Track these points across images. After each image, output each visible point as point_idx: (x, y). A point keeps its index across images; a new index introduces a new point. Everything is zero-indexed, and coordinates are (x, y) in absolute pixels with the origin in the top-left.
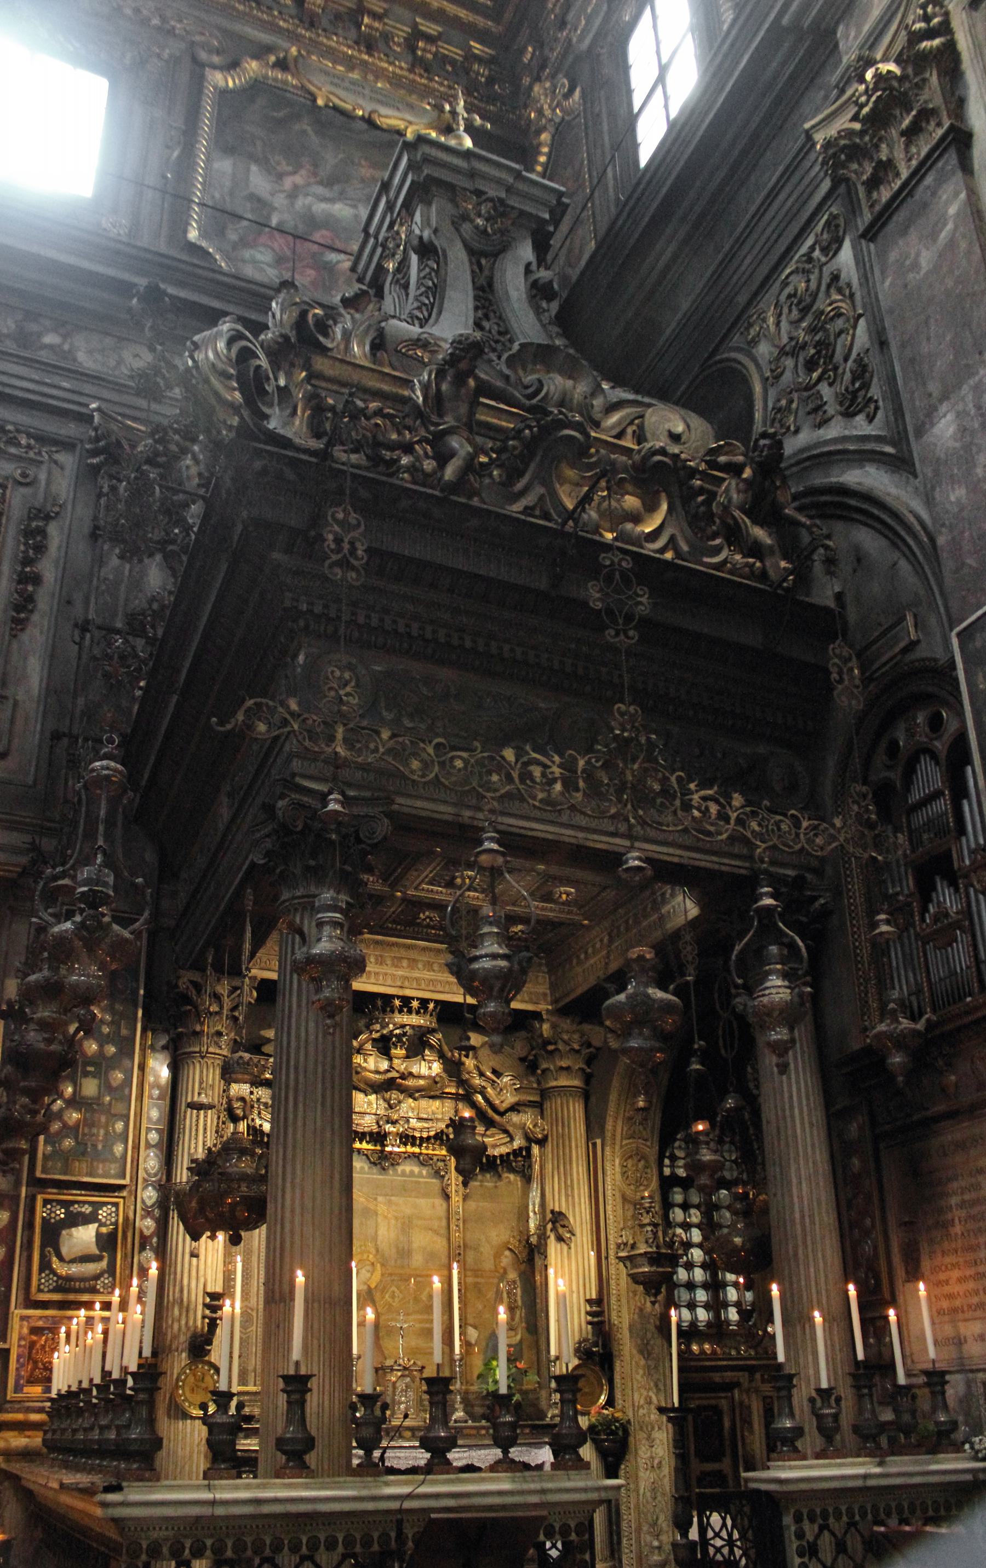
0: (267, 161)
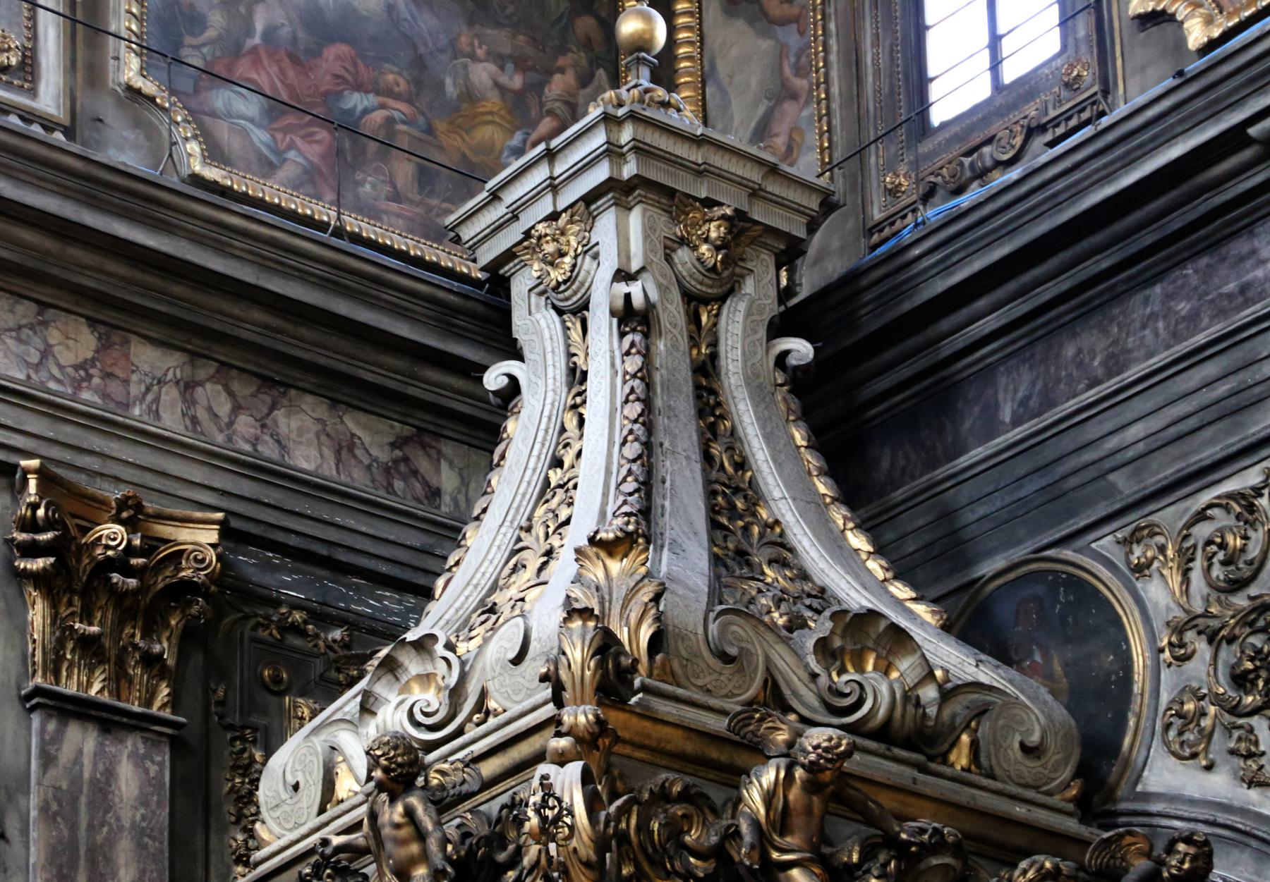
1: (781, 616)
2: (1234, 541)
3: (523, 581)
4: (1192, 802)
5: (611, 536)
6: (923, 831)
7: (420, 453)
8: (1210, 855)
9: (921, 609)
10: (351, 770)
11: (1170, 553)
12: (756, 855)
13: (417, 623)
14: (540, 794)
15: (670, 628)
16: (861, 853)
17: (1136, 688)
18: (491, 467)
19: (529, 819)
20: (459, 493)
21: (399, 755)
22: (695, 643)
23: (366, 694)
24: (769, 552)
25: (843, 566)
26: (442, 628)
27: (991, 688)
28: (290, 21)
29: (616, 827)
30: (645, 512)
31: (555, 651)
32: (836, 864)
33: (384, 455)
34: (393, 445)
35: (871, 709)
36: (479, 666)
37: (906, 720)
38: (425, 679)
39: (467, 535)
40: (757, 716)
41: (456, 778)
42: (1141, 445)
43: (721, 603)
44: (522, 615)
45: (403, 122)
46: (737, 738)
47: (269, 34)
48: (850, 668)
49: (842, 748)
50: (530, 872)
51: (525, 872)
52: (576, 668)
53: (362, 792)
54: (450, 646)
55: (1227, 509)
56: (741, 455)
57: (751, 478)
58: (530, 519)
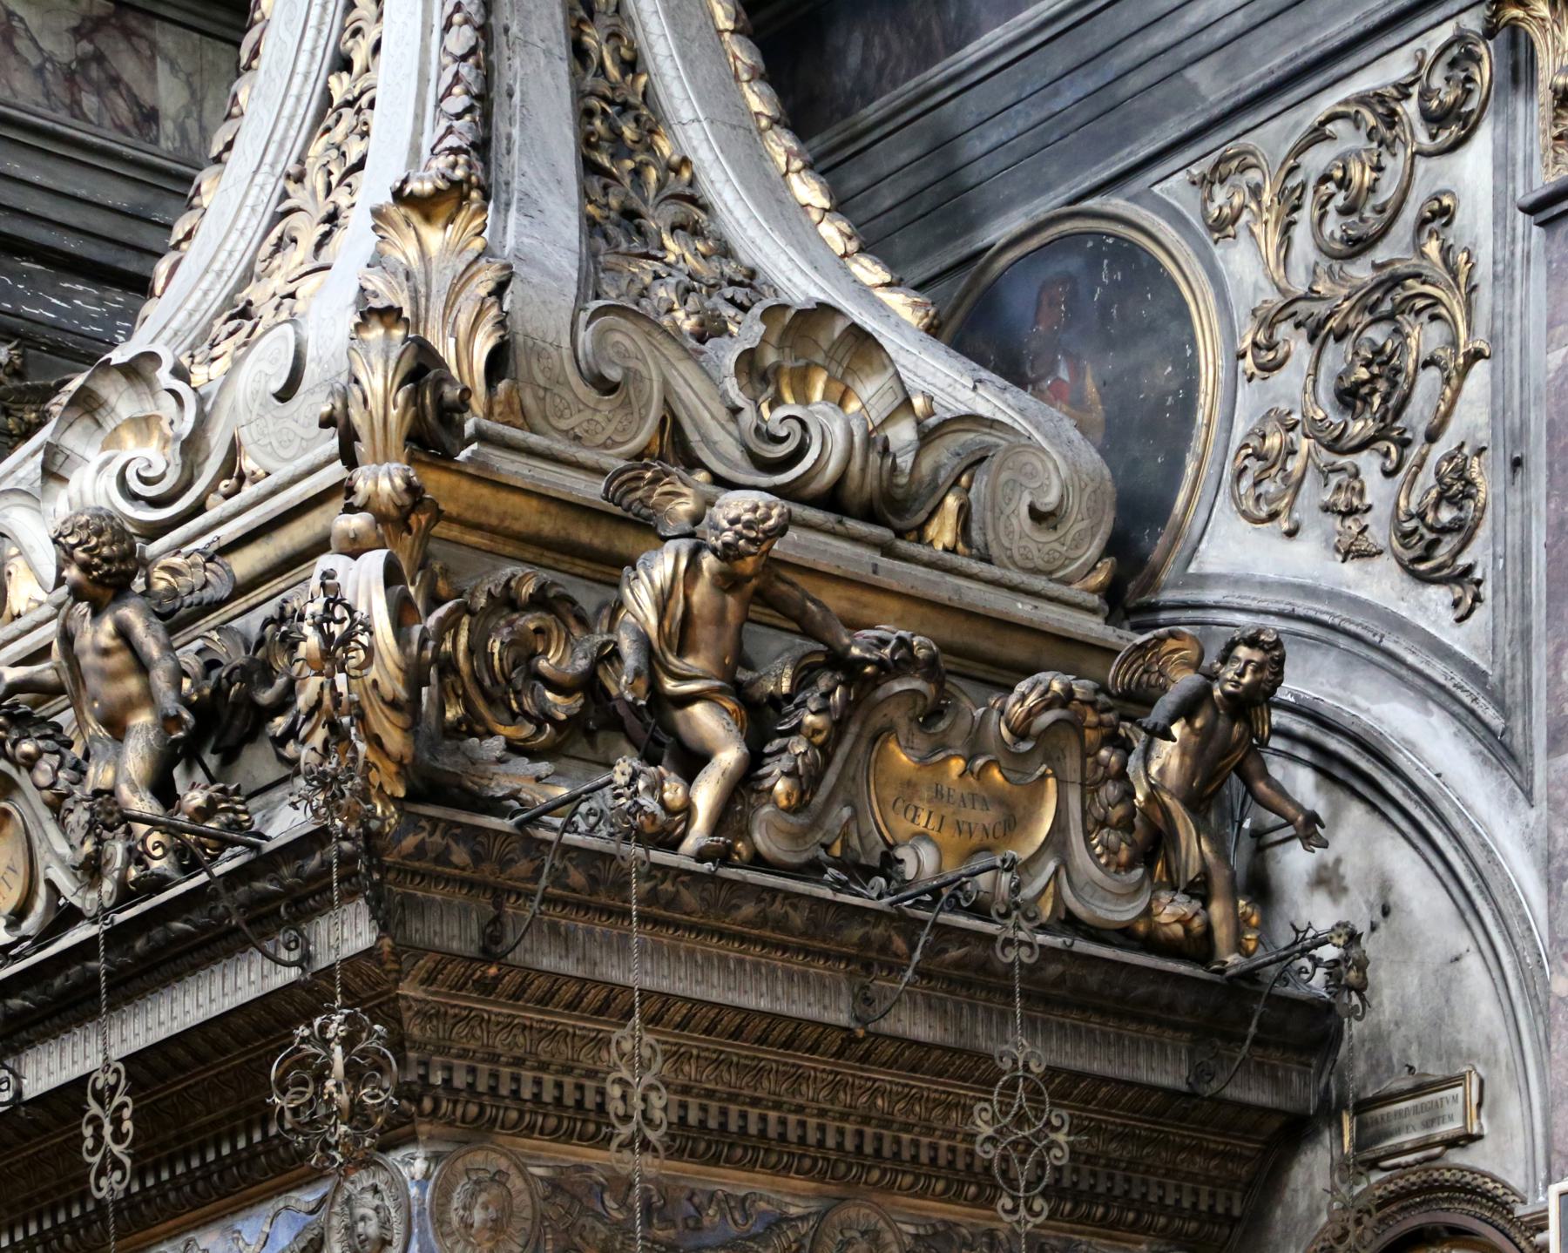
1: (688, 316)
2: (1360, 175)
3: (292, 265)
4: (1264, 585)
5: (428, 187)
6: (883, 642)
7: (122, 46)
8: (1280, 662)
9: (898, 301)
10: (31, 568)
11: (1266, 197)
12: (642, 686)
13: (129, 335)
14: (323, 600)
15: (520, 338)
16: (793, 679)
17: (1201, 417)
18: (238, 71)
19: (305, 639)
20: (188, 115)
21: (104, 544)
22: (558, 364)
23: (51, 450)
24: (672, 212)
25: (783, 234)
26: (167, 344)
27: (992, 423)
29: (437, 648)
30: (482, 147)
31: (344, 379)
32: (757, 695)
33: (63, 50)
34: (78, 33)
35: (817, 461)
36: (226, 404)
37: (865, 481)
38: (144, 424)
39: (203, 189)
40: (648, 475)
41: (197, 578)
42: (1239, 16)
43: (597, 297)
44: (292, 320)
46: (618, 510)
48: (788, 396)
49: (771, 522)
50: (309, 716)
51: (302, 717)
52: (376, 404)
53: (49, 602)
54: (180, 373)
55: (1356, 120)
56: (631, 48)
57: (646, 86)
58: (301, 161)
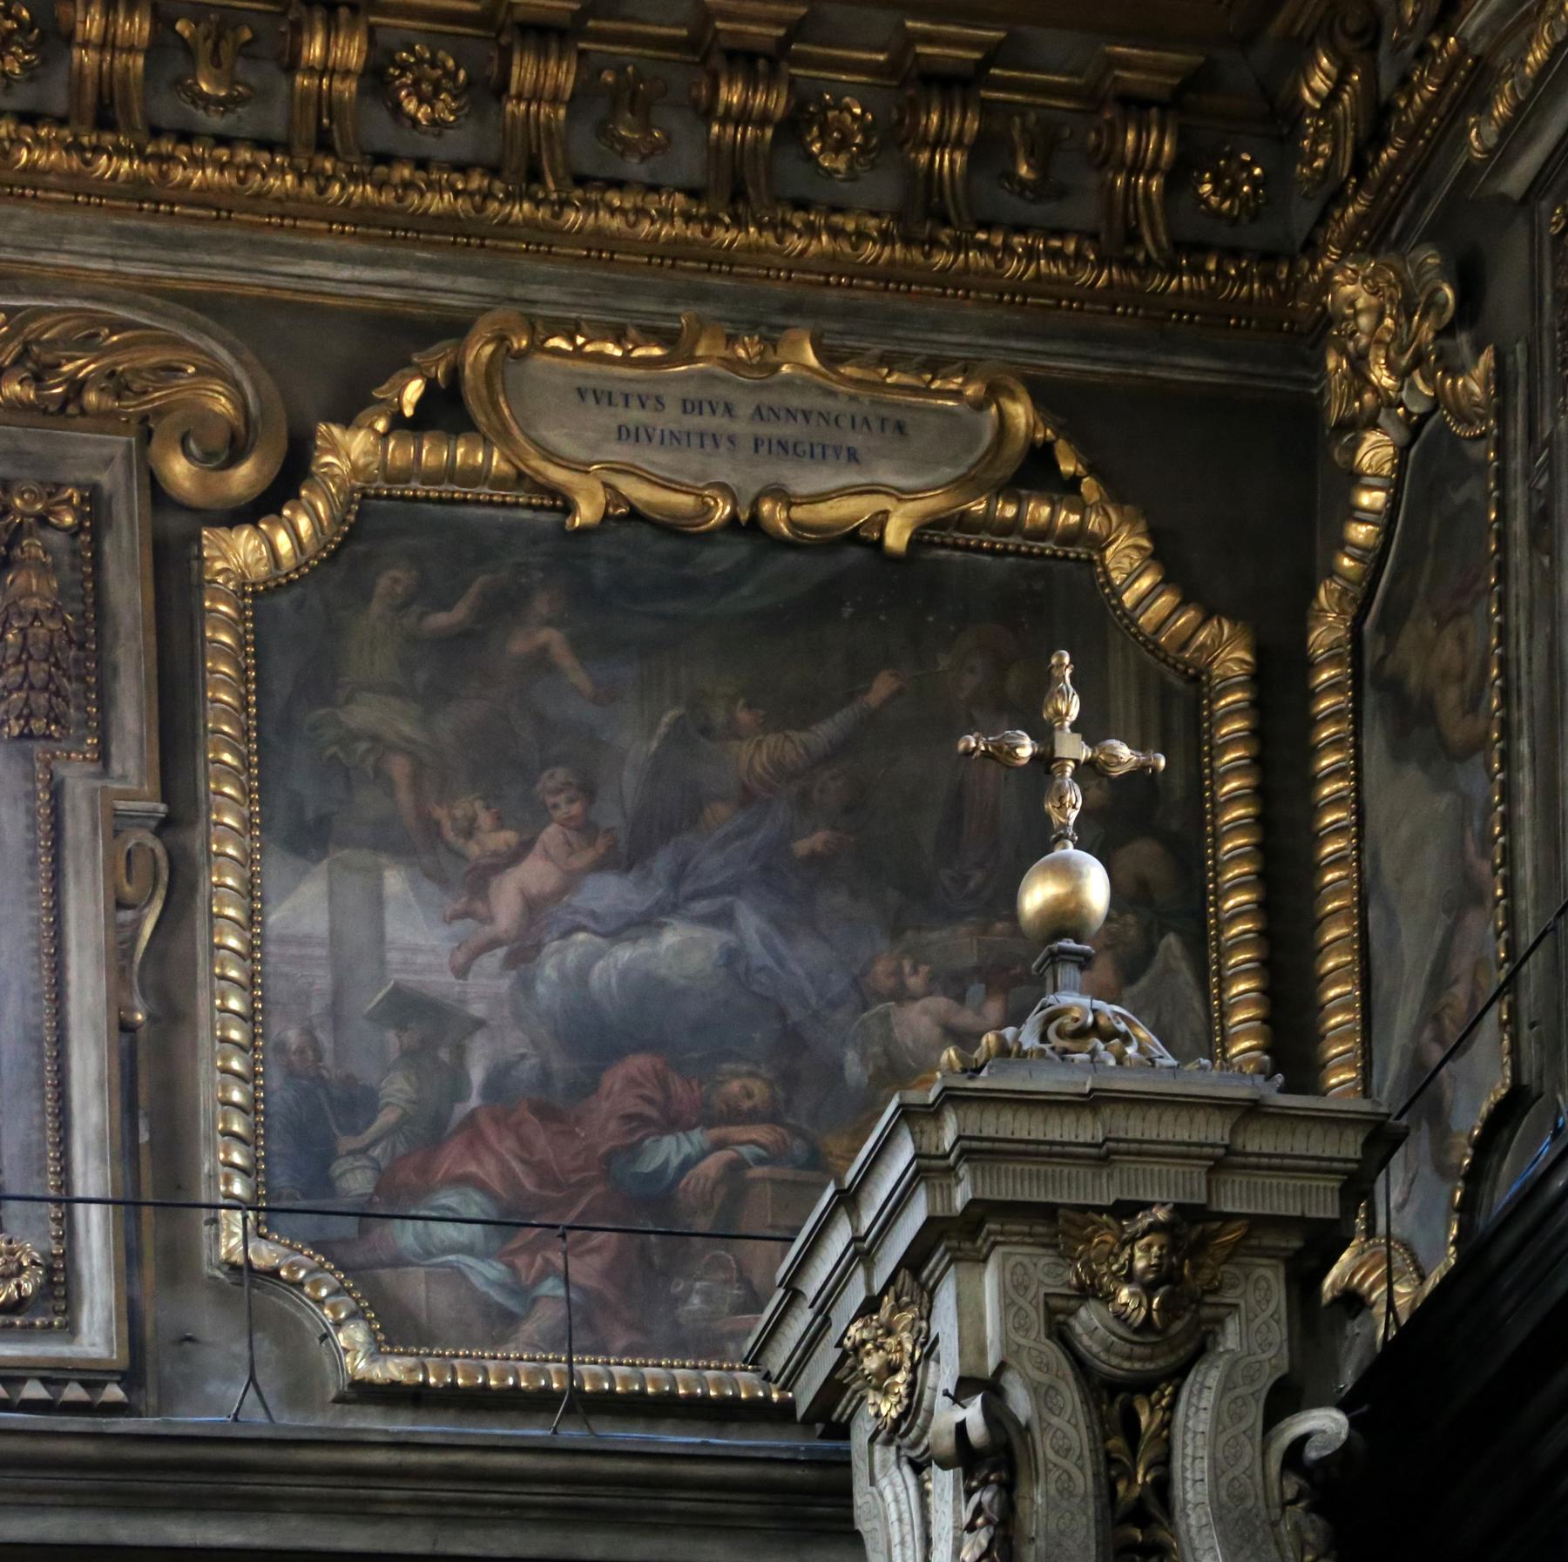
0: (432, 830)
28: (535, 1044)
45: (760, 1161)
47: (496, 1085)
